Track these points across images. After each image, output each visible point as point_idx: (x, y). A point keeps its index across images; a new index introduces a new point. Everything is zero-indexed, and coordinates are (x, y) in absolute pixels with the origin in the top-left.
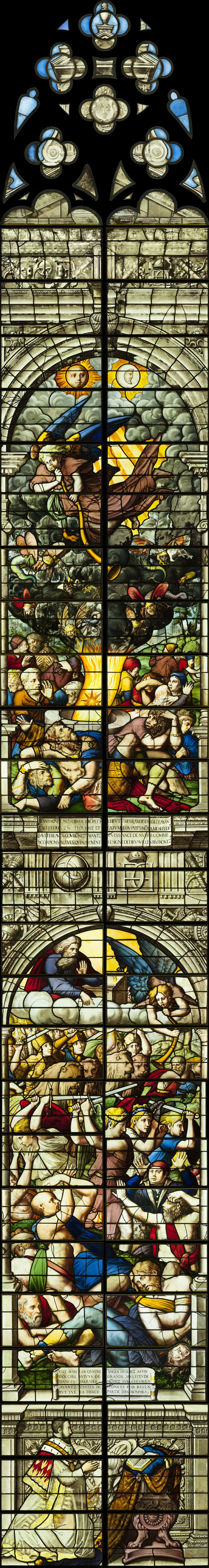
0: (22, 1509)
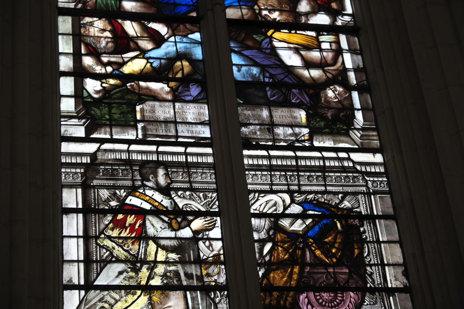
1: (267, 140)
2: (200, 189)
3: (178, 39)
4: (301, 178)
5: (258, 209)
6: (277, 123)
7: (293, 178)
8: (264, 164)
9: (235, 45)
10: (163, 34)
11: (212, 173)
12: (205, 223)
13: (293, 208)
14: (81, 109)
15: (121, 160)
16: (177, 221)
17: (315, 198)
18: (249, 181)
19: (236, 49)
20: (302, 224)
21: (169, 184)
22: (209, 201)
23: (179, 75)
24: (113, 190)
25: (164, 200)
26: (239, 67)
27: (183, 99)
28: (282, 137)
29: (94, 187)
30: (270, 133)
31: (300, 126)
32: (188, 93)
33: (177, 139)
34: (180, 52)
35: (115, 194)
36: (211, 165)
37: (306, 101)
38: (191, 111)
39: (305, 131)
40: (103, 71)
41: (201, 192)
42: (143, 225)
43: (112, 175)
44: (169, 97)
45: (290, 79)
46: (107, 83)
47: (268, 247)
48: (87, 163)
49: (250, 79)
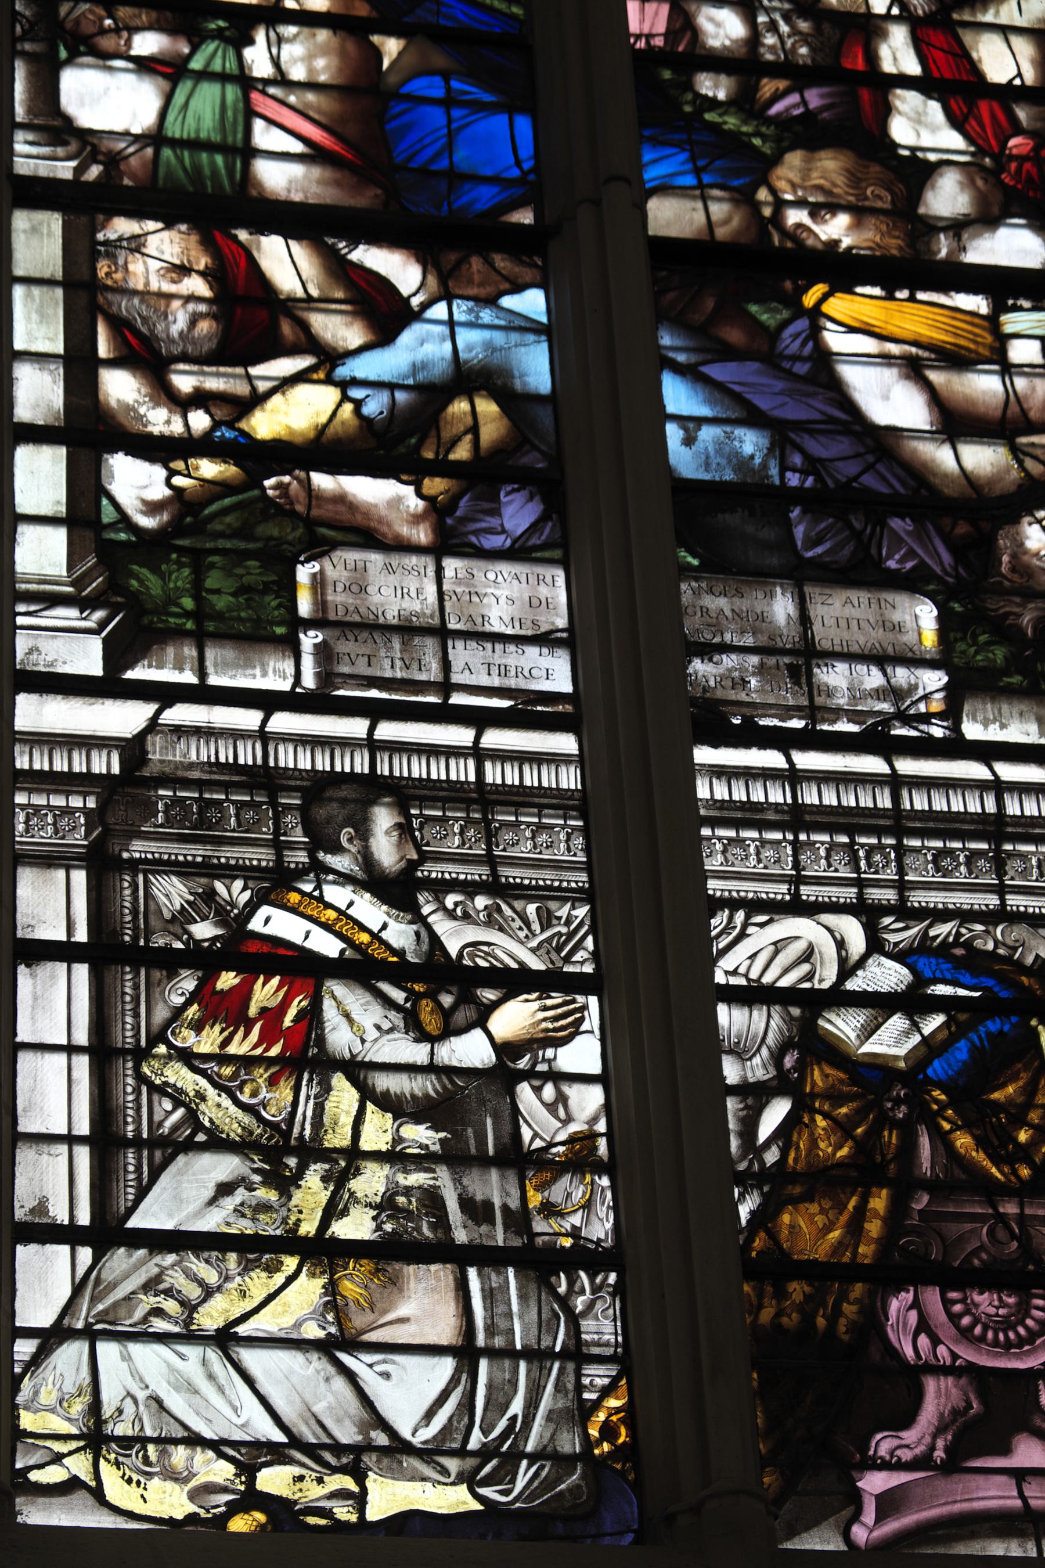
0: (135, 1222)
1: (788, 711)
2: (529, 887)
3: (461, 310)
4: (908, 860)
5: (742, 970)
6: (826, 645)
7: (877, 858)
8: (772, 800)
9: (678, 343)
10: (405, 290)
11: (574, 829)
12: (542, 1015)
13: (877, 970)
14: (91, 569)
15: (235, 767)
16: (439, 1004)
17: (958, 935)
18: (714, 863)
19: (681, 358)
20: (907, 1034)
21: (412, 866)
22: (559, 934)
23: (462, 452)
24: (203, 880)
25: (392, 923)
26: (691, 425)
27: (472, 545)
28: (842, 701)
29: (134, 866)
30: (797, 682)
31: (915, 661)
32: (493, 522)
33: (447, 697)
34: (466, 362)
35: (210, 895)
36: (570, 798)
37: (941, 563)
38: (503, 593)
39: (934, 680)
40: (177, 427)
41: (531, 899)
42: (312, 1016)
43: (202, 824)
44: (422, 535)
45: (884, 479)
46: (189, 476)
47: (775, 1113)
48: (109, 776)
49: (729, 476)
